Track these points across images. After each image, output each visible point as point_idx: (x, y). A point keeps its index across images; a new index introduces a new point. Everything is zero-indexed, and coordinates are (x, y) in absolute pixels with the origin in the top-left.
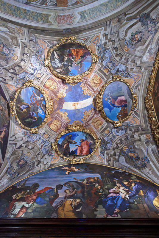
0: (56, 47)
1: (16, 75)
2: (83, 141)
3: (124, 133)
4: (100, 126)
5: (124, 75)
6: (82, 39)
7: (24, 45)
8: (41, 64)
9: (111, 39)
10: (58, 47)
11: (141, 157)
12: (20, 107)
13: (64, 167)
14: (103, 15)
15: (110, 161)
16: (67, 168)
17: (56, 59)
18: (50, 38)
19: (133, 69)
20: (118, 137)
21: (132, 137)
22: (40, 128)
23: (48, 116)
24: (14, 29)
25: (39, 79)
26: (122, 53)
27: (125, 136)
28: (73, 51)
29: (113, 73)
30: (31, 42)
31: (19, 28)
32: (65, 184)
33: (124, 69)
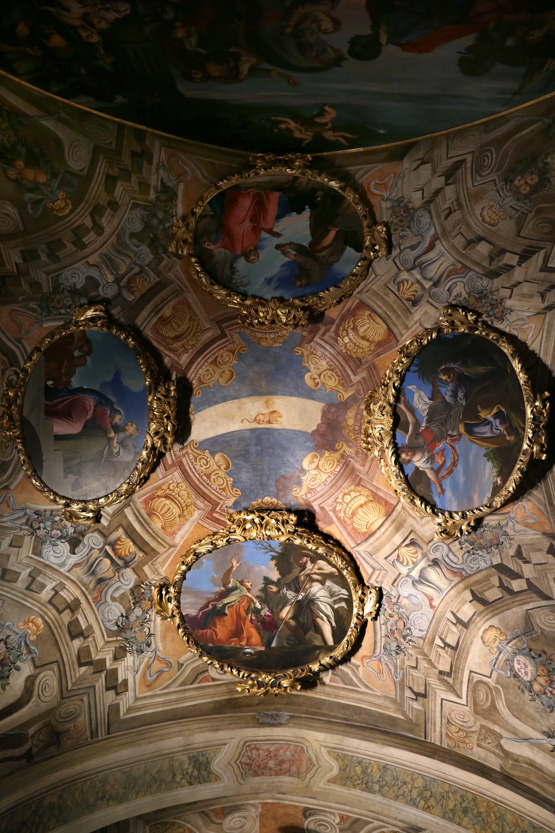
0: (323, 662)
1: (501, 564)
2: (246, 255)
3: (66, 273)
4: (167, 312)
5: (49, 523)
6: (214, 680)
7: (450, 680)
8: (394, 600)
9: (94, 673)
10: (315, 659)
12: (506, 429)
13: (343, 141)
14: (117, 764)
15: (134, 154)
16: (329, 135)
17: (330, 612)
18: (342, 697)
19: (11, 545)
20: (91, 260)
21: (29, 255)
22: (432, 330)
23: (389, 379)
24: (479, 745)
25: (408, 541)
26: (52, 612)
27: (60, 260)
28: (256, 638)
29: (96, 534)
30: (422, 690)
31: (461, 744)
32: (338, 61)
33: (47, 550)
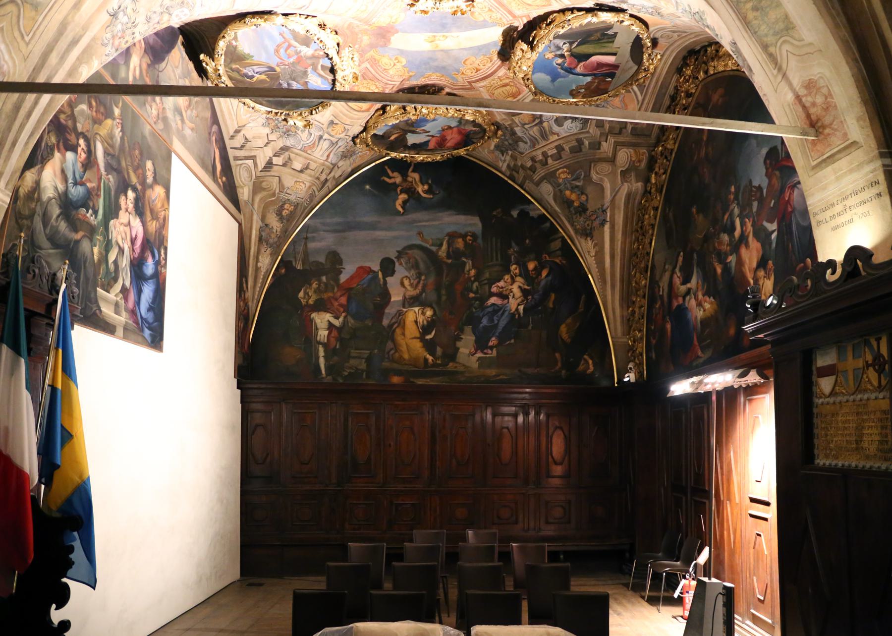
11: (591, 206)
32: (400, 254)
